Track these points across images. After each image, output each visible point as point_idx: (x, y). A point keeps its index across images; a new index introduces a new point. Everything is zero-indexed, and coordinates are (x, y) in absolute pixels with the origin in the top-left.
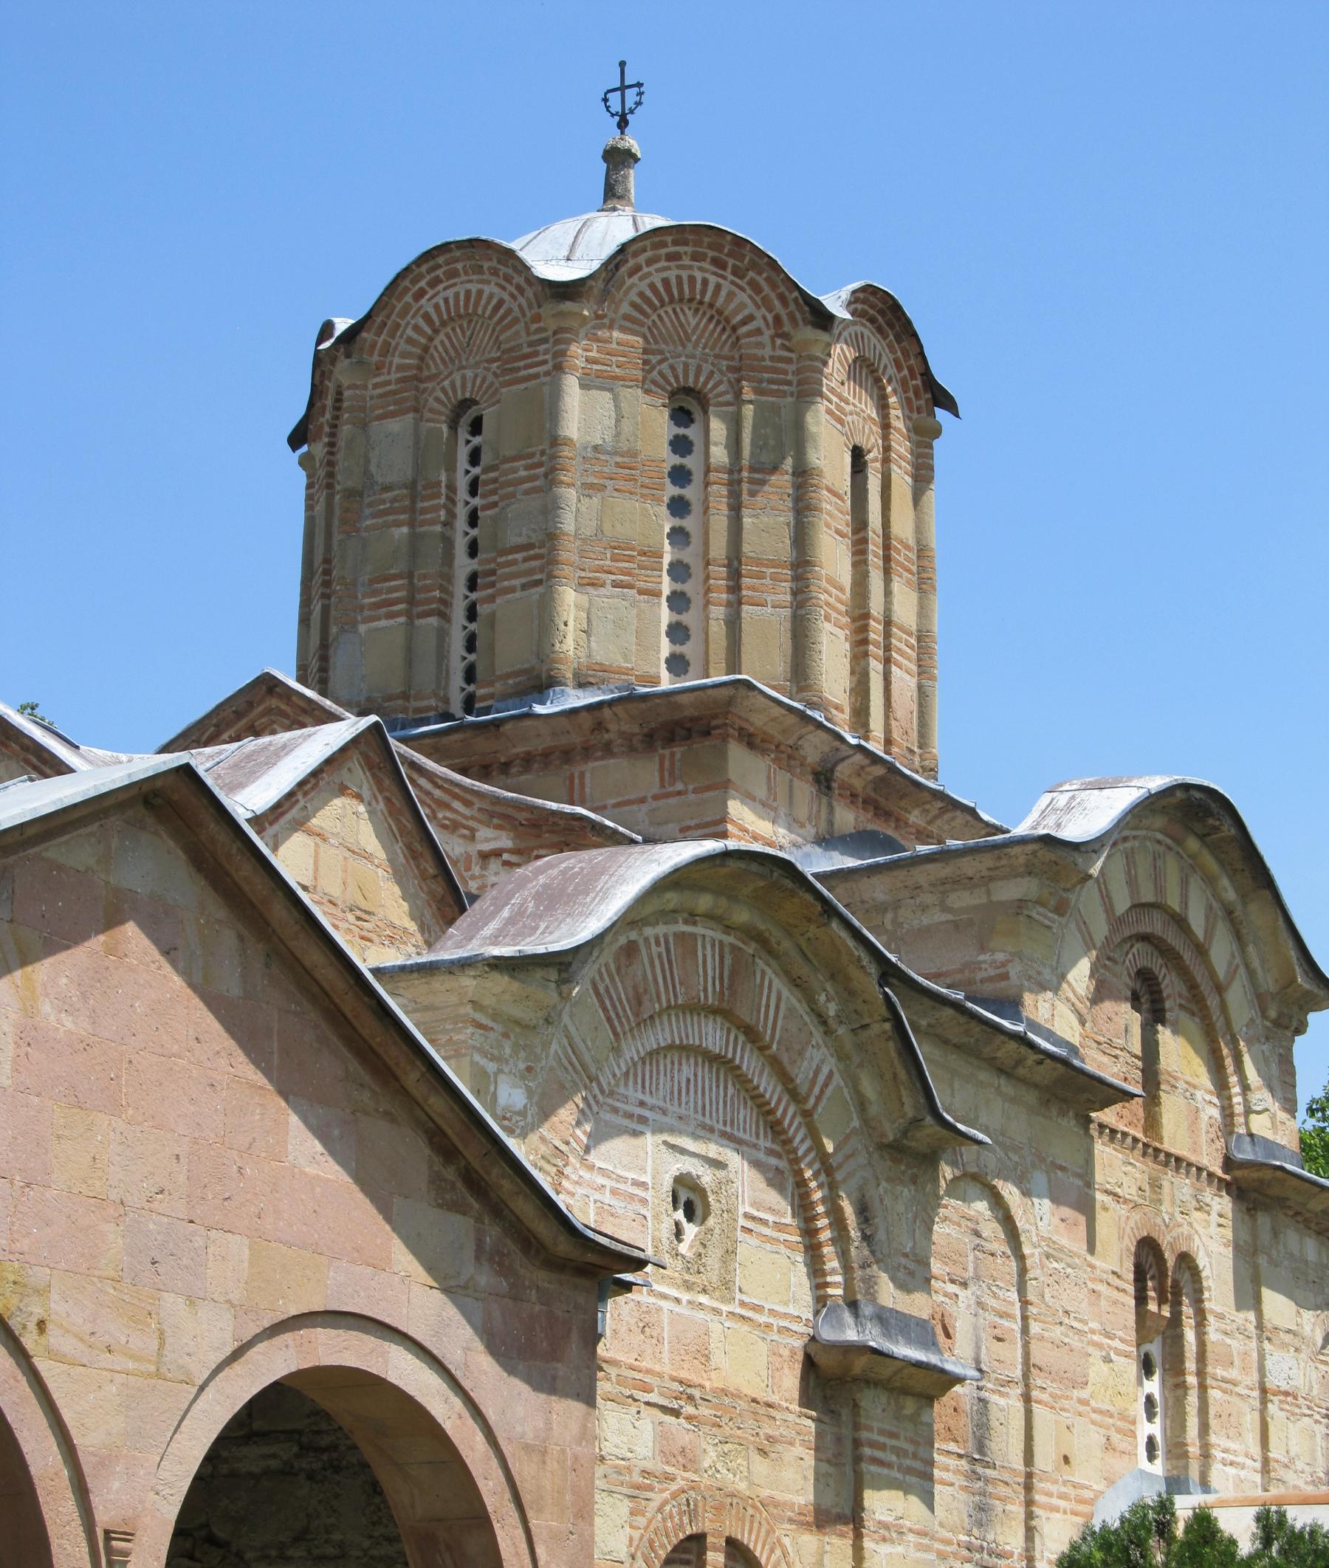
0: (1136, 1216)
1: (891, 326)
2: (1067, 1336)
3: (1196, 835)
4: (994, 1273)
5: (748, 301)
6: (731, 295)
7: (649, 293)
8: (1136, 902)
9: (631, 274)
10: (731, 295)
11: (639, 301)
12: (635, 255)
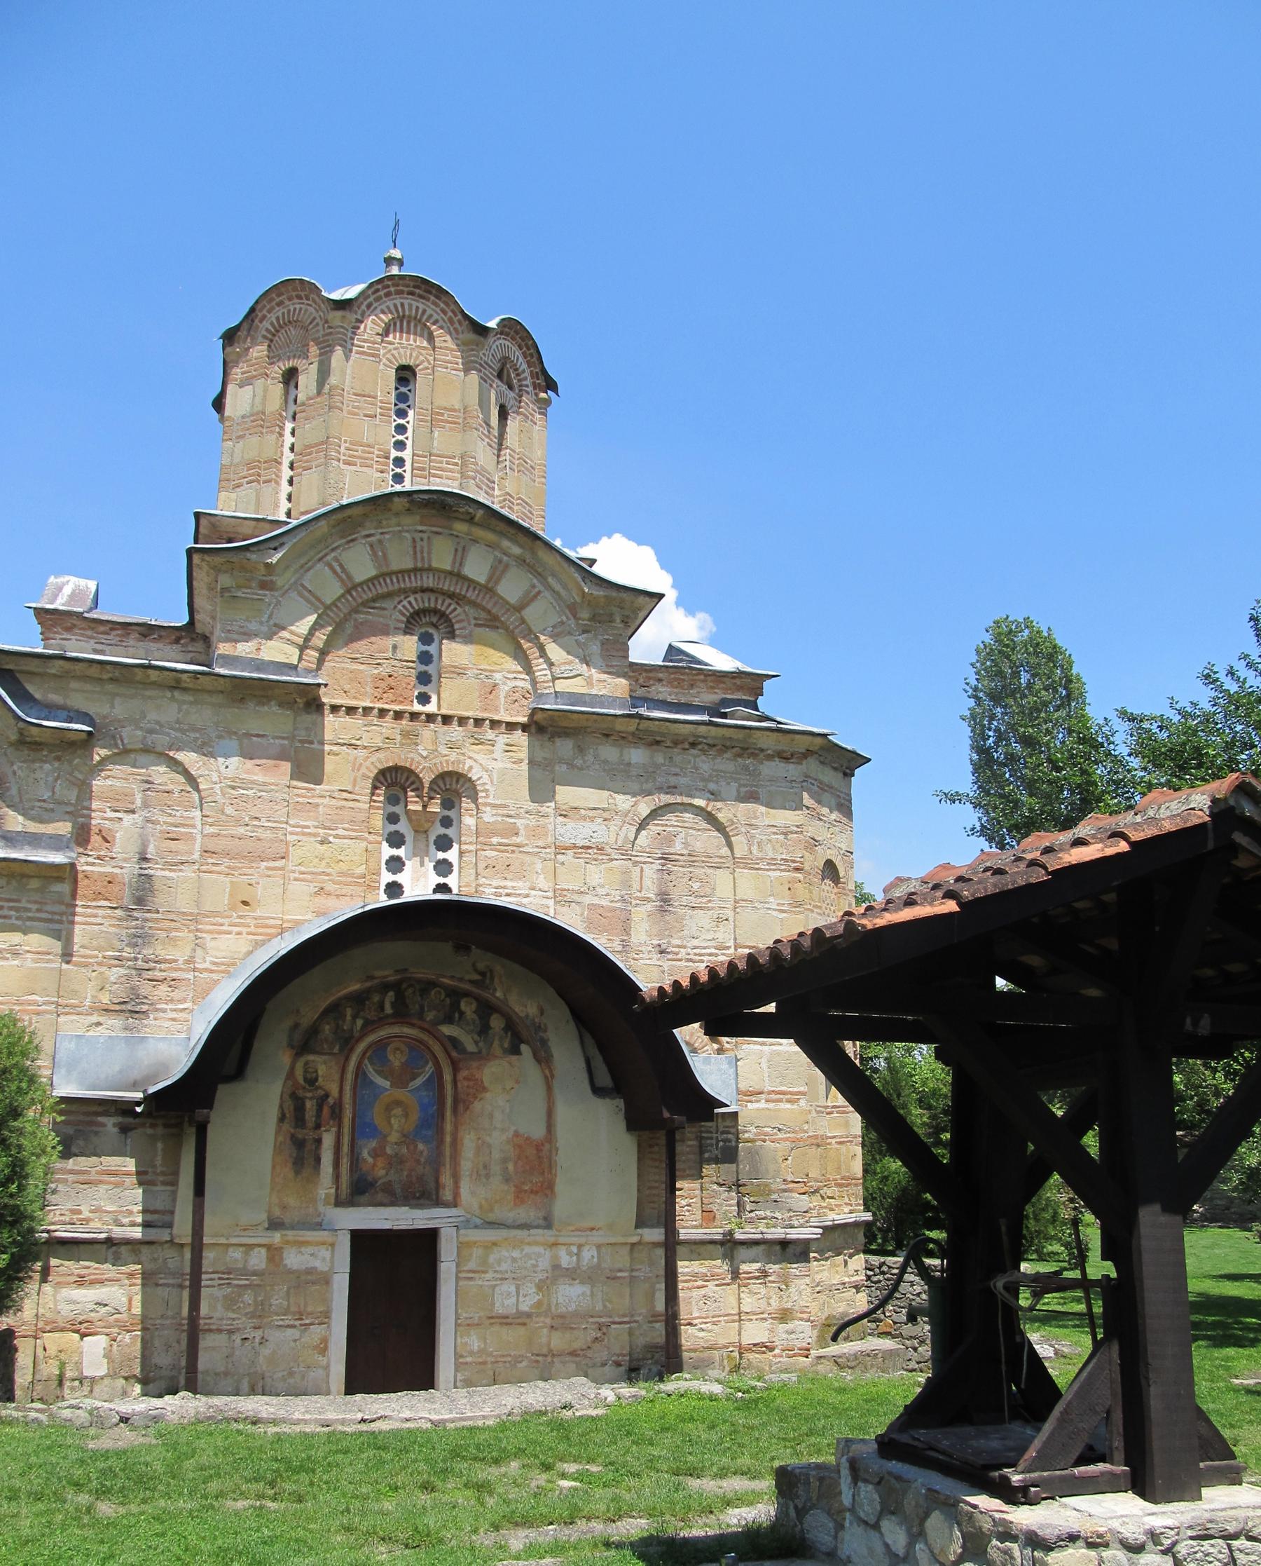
0: (380, 755)
1: (430, 293)
2: (253, 832)
3: (462, 520)
4: (169, 803)
5: (313, 311)
6: (306, 310)
7: (270, 328)
8: (385, 570)
9: (261, 321)
10: (306, 310)
11: (265, 333)
12: (261, 310)
